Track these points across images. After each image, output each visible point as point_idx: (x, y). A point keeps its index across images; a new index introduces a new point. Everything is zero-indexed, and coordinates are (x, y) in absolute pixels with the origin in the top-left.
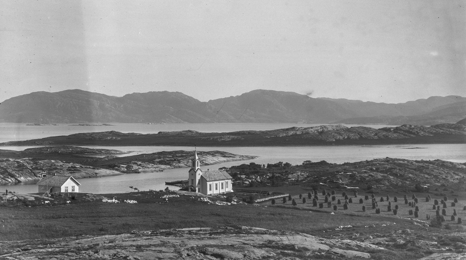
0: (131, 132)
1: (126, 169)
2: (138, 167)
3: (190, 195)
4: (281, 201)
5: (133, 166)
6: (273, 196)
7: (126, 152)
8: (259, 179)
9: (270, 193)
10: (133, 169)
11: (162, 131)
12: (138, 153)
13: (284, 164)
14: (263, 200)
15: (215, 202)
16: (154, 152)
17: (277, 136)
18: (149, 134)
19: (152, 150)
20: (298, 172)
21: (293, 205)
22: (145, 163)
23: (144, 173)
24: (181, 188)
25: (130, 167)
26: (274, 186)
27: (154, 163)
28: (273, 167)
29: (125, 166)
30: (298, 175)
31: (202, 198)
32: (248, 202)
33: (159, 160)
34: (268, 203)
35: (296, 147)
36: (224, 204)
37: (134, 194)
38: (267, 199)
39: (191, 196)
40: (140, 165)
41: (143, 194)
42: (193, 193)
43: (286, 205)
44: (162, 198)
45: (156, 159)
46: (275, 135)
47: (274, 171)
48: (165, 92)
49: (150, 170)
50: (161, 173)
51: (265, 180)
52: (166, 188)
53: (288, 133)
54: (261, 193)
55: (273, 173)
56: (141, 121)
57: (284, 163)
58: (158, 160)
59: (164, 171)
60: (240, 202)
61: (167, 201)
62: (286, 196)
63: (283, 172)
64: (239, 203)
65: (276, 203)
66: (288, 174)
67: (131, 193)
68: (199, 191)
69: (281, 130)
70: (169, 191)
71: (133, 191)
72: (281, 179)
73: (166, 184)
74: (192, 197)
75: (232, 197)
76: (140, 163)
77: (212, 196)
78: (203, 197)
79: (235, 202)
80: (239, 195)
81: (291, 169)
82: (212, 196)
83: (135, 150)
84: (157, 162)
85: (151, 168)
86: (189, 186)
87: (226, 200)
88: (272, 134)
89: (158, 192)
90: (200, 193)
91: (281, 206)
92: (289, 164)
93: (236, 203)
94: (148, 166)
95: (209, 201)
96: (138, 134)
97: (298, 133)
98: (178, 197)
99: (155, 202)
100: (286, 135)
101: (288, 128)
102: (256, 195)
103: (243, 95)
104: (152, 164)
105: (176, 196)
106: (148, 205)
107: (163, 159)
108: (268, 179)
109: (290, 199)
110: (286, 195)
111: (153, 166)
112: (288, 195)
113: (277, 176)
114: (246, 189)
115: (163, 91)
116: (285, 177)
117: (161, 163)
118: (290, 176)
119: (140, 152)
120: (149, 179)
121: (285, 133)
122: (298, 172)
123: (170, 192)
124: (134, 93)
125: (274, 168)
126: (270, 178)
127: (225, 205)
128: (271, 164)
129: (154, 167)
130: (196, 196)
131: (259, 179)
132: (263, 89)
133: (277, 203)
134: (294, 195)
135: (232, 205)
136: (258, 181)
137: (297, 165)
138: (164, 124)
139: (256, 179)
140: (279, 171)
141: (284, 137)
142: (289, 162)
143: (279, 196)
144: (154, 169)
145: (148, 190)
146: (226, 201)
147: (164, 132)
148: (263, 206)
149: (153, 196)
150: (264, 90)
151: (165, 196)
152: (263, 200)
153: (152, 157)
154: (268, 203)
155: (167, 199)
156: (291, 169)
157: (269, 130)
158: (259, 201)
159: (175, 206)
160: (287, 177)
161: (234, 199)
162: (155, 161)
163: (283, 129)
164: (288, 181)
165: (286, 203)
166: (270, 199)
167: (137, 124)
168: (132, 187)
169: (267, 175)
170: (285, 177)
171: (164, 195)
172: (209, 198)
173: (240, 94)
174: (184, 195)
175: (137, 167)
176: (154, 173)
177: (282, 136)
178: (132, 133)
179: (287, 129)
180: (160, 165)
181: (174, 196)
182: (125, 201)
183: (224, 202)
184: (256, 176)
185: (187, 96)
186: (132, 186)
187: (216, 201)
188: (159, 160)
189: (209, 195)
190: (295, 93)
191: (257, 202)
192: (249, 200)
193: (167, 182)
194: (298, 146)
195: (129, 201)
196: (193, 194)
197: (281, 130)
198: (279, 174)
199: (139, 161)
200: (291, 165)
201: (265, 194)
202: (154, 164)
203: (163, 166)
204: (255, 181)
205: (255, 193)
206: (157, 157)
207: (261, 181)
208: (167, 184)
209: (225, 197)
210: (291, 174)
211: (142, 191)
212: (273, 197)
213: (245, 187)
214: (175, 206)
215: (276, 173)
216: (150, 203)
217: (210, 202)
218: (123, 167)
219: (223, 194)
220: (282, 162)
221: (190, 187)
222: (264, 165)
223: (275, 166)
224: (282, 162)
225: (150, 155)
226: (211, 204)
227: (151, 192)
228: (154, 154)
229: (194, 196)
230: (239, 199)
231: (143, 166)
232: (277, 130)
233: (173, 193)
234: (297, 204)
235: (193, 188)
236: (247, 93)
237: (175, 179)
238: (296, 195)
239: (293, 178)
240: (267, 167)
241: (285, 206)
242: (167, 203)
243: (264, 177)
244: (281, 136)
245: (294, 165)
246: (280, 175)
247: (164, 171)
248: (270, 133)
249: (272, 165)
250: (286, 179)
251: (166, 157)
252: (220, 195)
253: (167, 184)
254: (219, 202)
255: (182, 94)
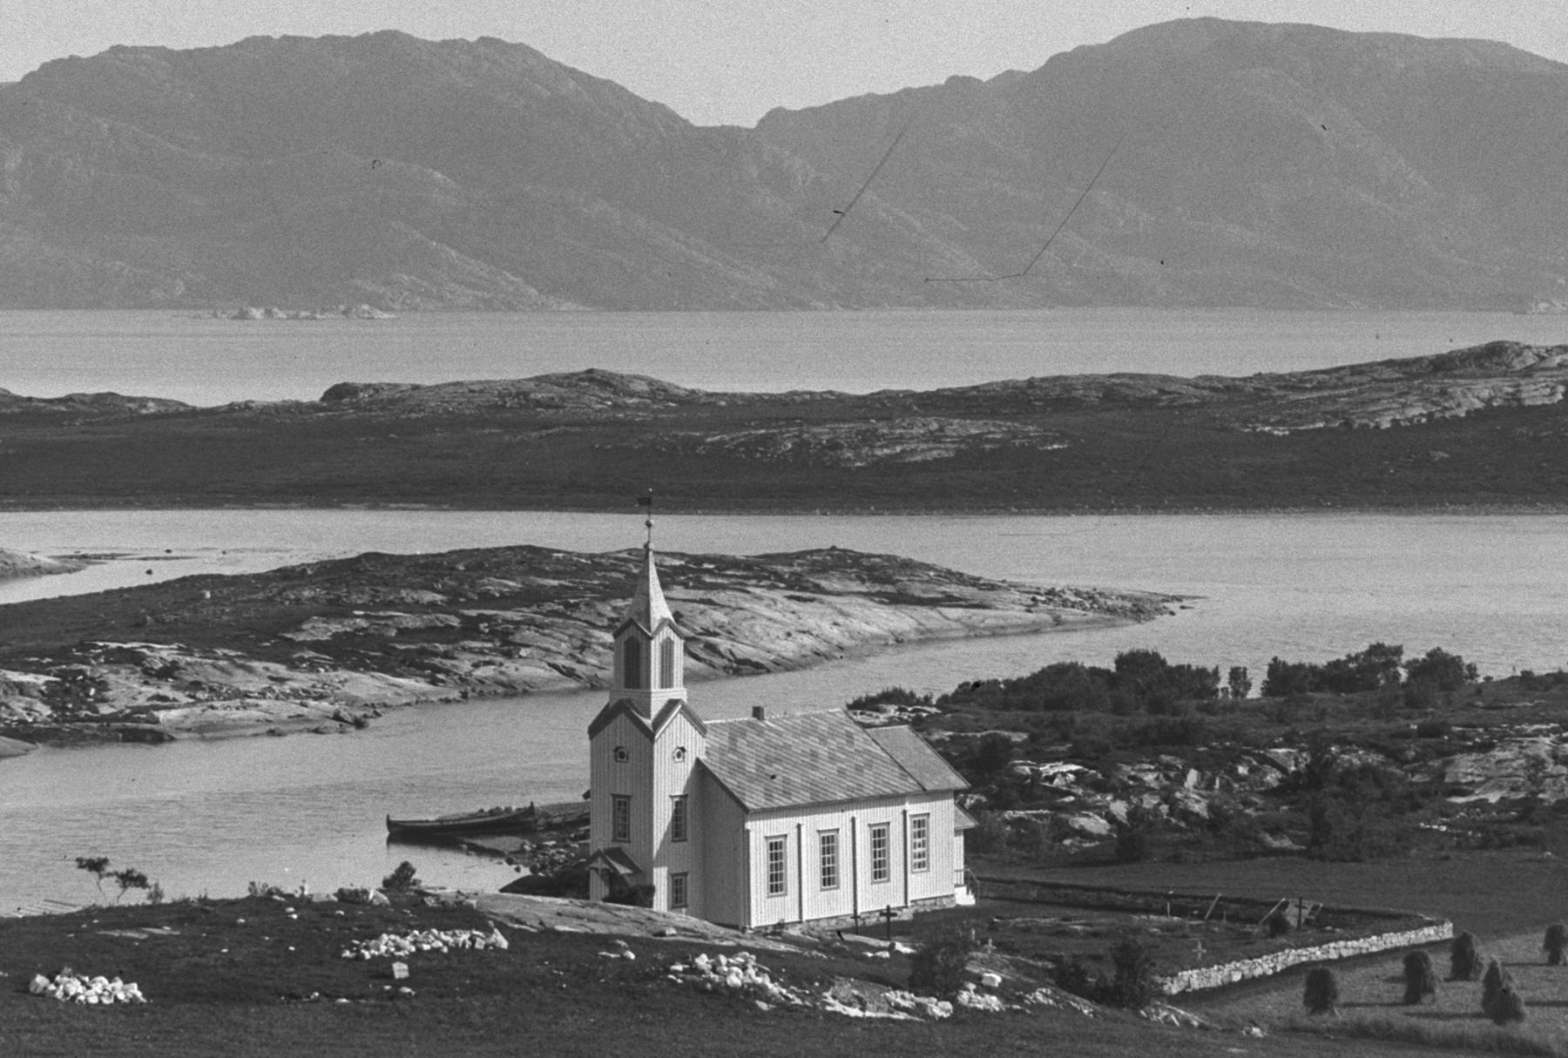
0: (91, 390)
1: (46, 711)
2: (151, 691)
3: (601, 929)
4: (1382, 987)
5: (111, 678)
6: (1320, 944)
7: (44, 559)
8: (1193, 793)
9: (1291, 918)
10: (105, 710)
11: (359, 378)
12: (149, 565)
13: (1408, 665)
14: (1234, 972)
15: (815, 997)
16: (292, 561)
17: (1348, 424)
18: (247, 406)
19: (267, 545)
20: (1530, 729)
21: (1487, 1022)
22: (208, 653)
23: (203, 745)
24: (526, 872)
25: (85, 688)
26: (1322, 858)
27: (286, 654)
28: (1318, 688)
29: (42, 679)
30: (1538, 763)
31: (703, 961)
32: (1100, 995)
33: (335, 627)
34: (1273, 1004)
35: (1515, 520)
36: (898, 1008)
37: (115, 926)
38: (1264, 966)
39: (607, 941)
40: (168, 672)
41: (192, 920)
42: (628, 911)
43: (1427, 1015)
44: (360, 958)
45: (307, 618)
46: (1335, 414)
47: (1330, 725)
48: (387, 39)
49: (254, 713)
50: (352, 742)
51: (1247, 804)
52: (389, 871)
53: (1443, 393)
54: (1217, 915)
55: (1317, 745)
56: (180, 289)
57: (1415, 651)
58: (321, 630)
59: (372, 723)
60: (1031, 989)
61: (404, 982)
62: (1432, 945)
63: (1406, 735)
64: (1020, 1000)
65: (1342, 999)
66: (1445, 754)
67: (89, 913)
68: (677, 901)
69: (1388, 374)
70: (422, 894)
71: (109, 894)
72: (1386, 797)
73: (391, 840)
74: (615, 949)
75: (967, 946)
76: (165, 653)
77: (789, 940)
78: (713, 951)
79: (990, 990)
80: (1027, 930)
81: (1471, 705)
82: (789, 940)
83: (125, 545)
84: (317, 646)
85: (263, 695)
86: (593, 858)
87: (907, 972)
88: (1306, 404)
89: (324, 908)
90: (683, 918)
91: (1390, 1025)
92: (1455, 662)
93: (994, 1002)
94: (240, 680)
95: (763, 988)
96: (152, 408)
97: (1536, 394)
98: (497, 949)
99: (299, 991)
100: (1430, 415)
101: (1444, 348)
102: (1167, 928)
103: (1058, 63)
104: (273, 666)
105: (480, 945)
106: (235, 1014)
107: (363, 623)
108: (1270, 793)
109: (1464, 964)
110: (1429, 934)
111: (281, 680)
112: (1447, 931)
113: (1349, 772)
114: (1083, 878)
115: (371, 30)
116: (1417, 778)
117: (347, 653)
118: (1465, 767)
119: (168, 556)
120: (243, 797)
121: (1425, 398)
122: (1538, 733)
123: (430, 902)
124: (117, 50)
125: (1324, 697)
126: (1290, 787)
127: (902, 1016)
128: (1300, 667)
129: (287, 688)
130: (653, 945)
131: (1193, 793)
132: (1232, 17)
133: (1346, 1005)
134: (1500, 933)
135: (963, 1015)
136: (1186, 814)
137: (1527, 675)
138: (379, 314)
139: (1167, 797)
140: (1372, 726)
141: (1414, 426)
142: (1451, 650)
143: (1373, 944)
144: (293, 708)
145: (241, 892)
146: (914, 986)
147: (377, 389)
148: (1231, 1029)
149: (281, 943)
150: (1243, 27)
151: (385, 943)
152: (1234, 972)
153: (270, 600)
154: (1273, 1004)
155: (400, 970)
156: (1471, 705)
157: (1284, 369)
158: (1196, 984)
159: (469, 1025)
160: (1443, 776)
161: (982, 963)
162: (301, 637)
163: (1404, 363)
164: (1446, 812)
165: (1426, 999)
166: (1290, 971)
167: (139, 320)
168: (96, 866)
169: (1264, 760)
170: (1417, 778)
171: (377, 936)
172: (763, 956)
173: (1032, 62)
174: (548, 934)
175: (144, 693)
176: (288, 738)
177: (1395, 421)
178: (99, 398)
179: (1439, 357)
180: (343, 674)
181: (464, 937)
182: (40, 980)
183: (895, 996)
184: (1169, 767)
185: (572, 71)
186: (95, 856)
187: (827, 985)
188: (335, 627)
189: (761, 932)
190: (1505, 46)
191: (1183, 993)
192: (1111, 975)
193: (398, 817)
194: (1531, 504)
195: (75, 987)
196: (622, 920)
197: (1388, 374)
198: (1371, 747)
199: (165, 634)
200: (1472, 669)
201: (1252, 921)
202: (293, 665)
203: (366, 685)
204: (1164, 808)
205: (1162, 912)
206: (314, 599)
207: (1210, 808)
208: (402, 834)
209: (899, 946)
210: (1469, 750)
211: (186, 902)
212: (1317, 953)
213: (1074, 865)
214: (469, 1025)
215: (1342, 742)
216: (258, 1002)
217: (774, 988)
218: (21, 689)
219: (888, 925)
220: (1398, 651)
221: (600, 864)
222: (1238, 675)
223: (1336, 677)
224: (1398, 651)
225: (256, 590)
226: (784, 1007)
227: (264, 903)
228: (287, 576)
229: (633, 942)
230: (1028, 970)
231: (197, 685)
232: (1356, 370)
233: (458, 913)
234: (1525, 1010)
235: (623, 870)
236: (1091, 49)
237: (470, 790)
238: (1520, 929)
239: (1489, 781)
240: (1268, 689)
241: (1425, 1023)
242: (400, 1004)
243: (1240, 779)
244: (1386, 424)
245: (1501, 672)
246: (1374, 759)
247: (372, 723)
248: (1293, 396)
249: (1313, 669)
250: (1425, 794)
251: (390, 605)
252: (855, 930)
253: (402, 834)
254: (848, 989)
255: (536, 54)
